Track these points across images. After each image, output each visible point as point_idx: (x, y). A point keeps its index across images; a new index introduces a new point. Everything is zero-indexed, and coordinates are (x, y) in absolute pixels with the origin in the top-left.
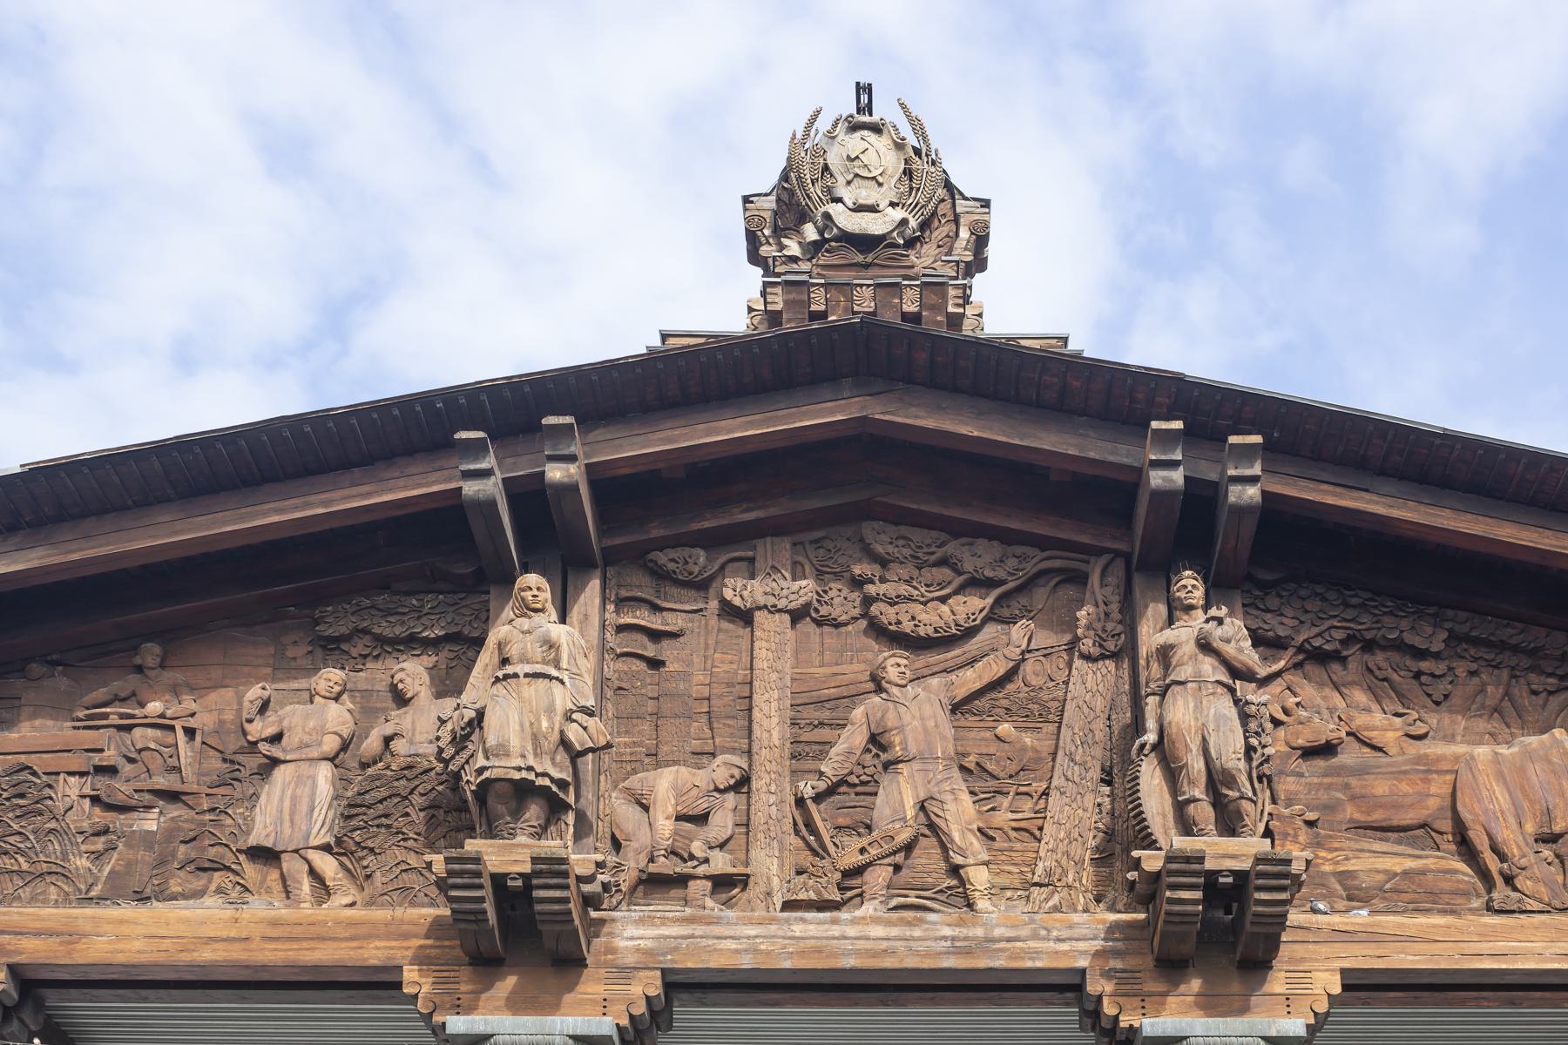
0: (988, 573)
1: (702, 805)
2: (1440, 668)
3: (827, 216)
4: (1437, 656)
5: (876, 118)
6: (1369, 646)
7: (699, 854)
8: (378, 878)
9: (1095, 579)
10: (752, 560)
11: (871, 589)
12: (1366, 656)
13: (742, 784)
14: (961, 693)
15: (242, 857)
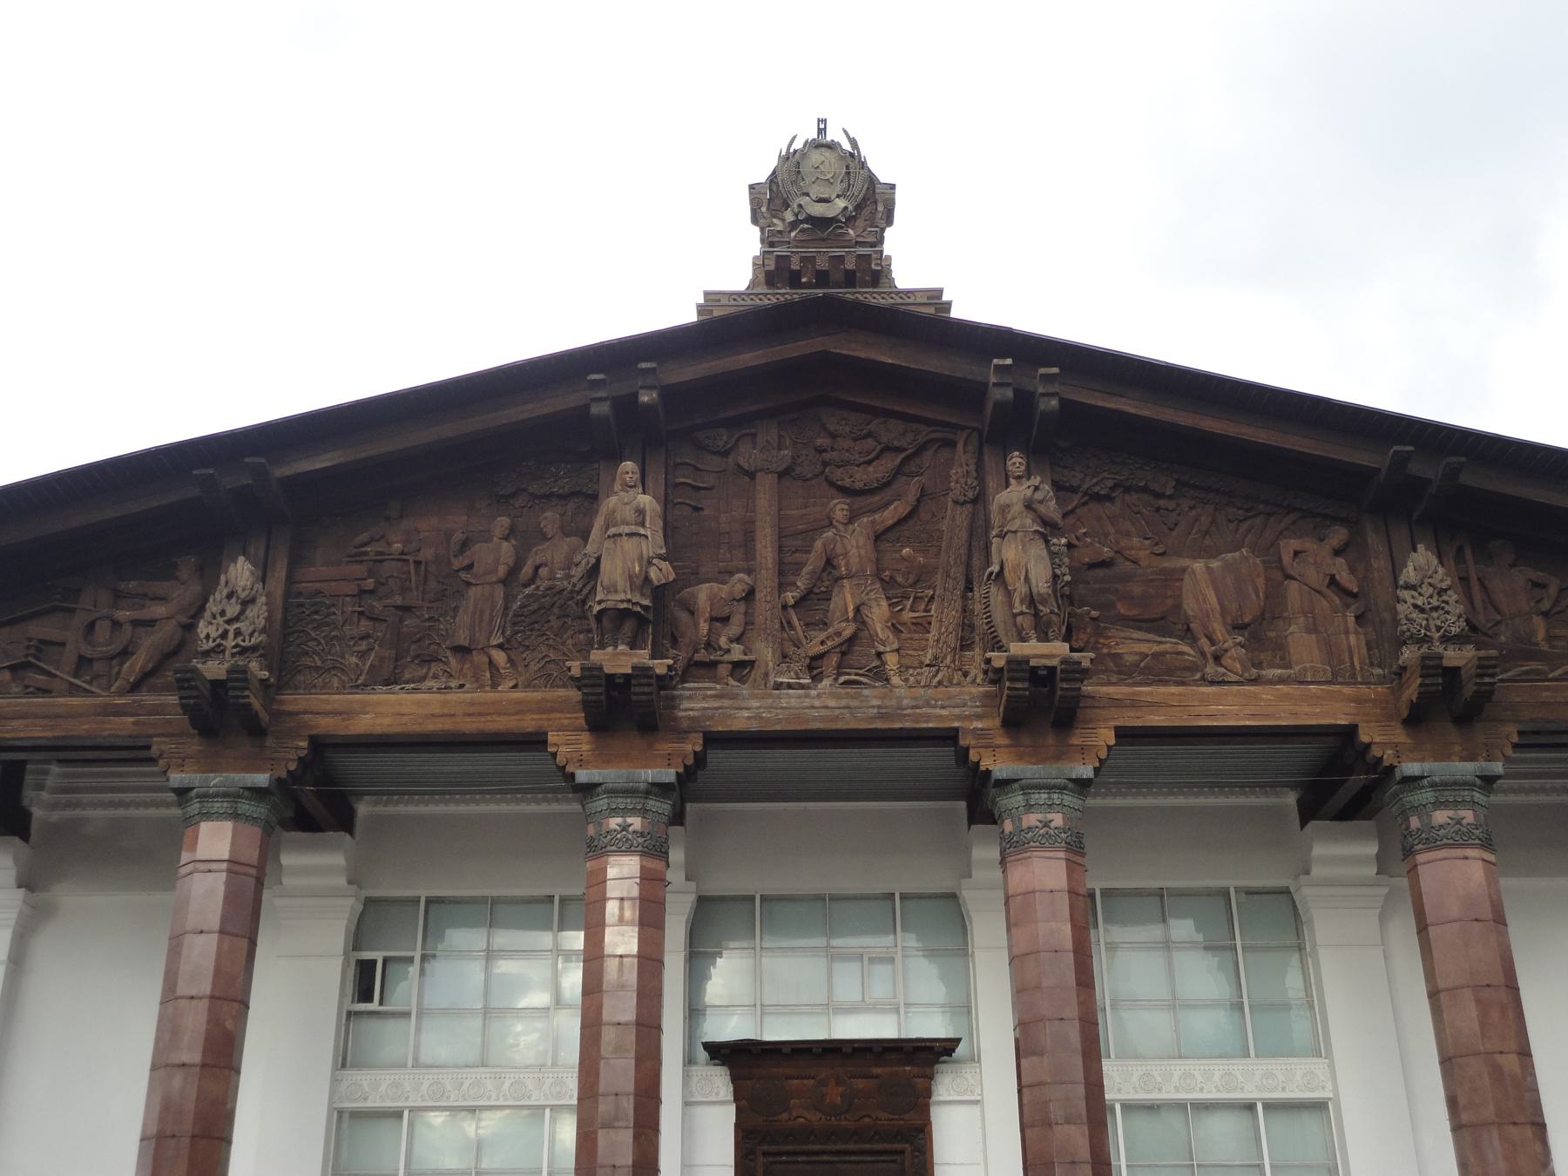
0: (896, 443)
1: (726, 611)
2: (1171, 504)
3: (800, 206)
4: (1170, 497)
5: (829, 138)
6: (1127, 490)
7: (725, 646)
8: (533, 667)
9: (960, 446)
10: (754, 435)
11: (827, 456)
12: (1127, 497)
13: (750, 595)
14: (880, 528)
15: (448, 653)
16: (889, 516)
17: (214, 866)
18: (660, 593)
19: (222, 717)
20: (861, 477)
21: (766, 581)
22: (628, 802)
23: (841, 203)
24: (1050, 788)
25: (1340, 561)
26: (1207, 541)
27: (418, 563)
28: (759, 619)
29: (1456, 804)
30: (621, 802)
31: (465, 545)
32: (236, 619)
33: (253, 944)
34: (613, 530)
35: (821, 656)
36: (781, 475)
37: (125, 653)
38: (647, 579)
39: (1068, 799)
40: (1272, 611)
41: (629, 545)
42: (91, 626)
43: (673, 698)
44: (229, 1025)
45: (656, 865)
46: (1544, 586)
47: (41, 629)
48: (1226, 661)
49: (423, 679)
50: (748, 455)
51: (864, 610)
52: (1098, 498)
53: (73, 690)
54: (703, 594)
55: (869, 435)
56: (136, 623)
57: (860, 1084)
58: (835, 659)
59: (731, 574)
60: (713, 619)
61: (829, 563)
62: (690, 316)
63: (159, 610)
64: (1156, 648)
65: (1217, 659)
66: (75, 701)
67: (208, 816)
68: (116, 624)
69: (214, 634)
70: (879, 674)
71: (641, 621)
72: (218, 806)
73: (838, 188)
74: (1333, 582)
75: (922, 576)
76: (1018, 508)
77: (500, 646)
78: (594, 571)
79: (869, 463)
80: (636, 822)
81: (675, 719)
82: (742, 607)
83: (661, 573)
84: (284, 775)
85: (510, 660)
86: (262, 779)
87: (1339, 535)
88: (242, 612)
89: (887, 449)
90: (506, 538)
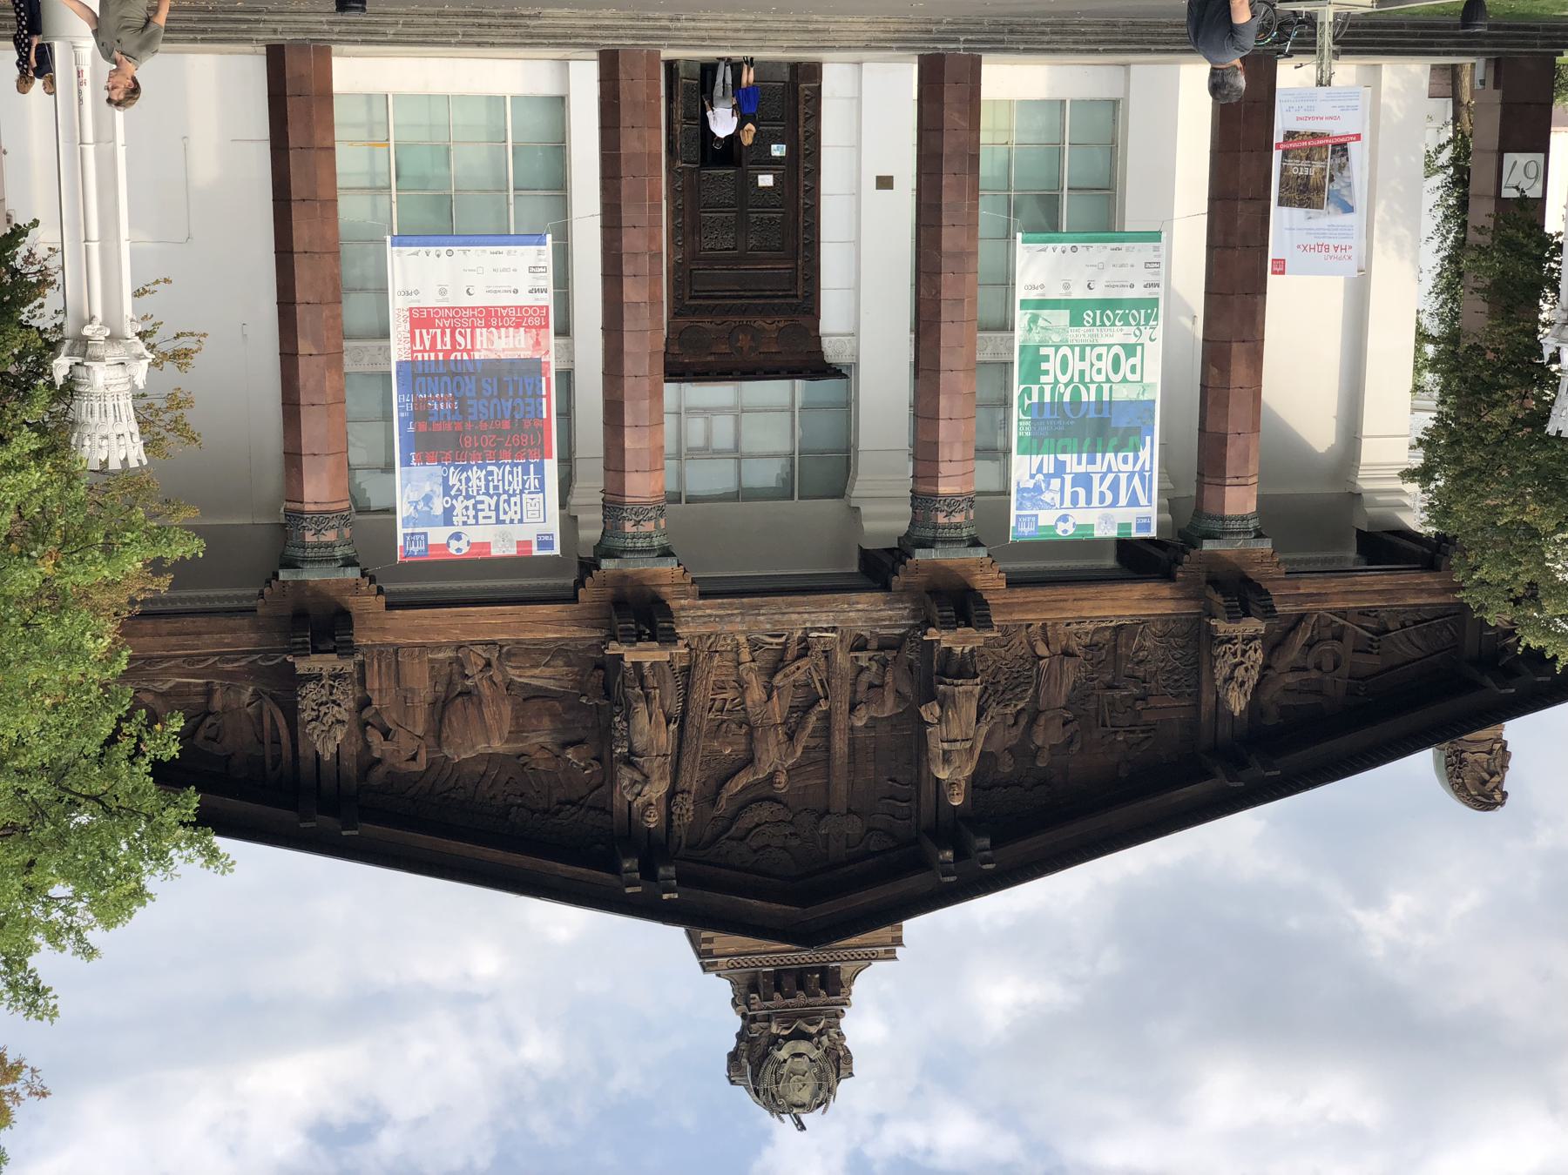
2: (510, 799)
6: (546, 811)
11: (791, 829)
16: (743, 780)
17: (1235, 481)
18: (930, 696)
19: (1240, 591)
20: (764, 812)
21: (840, 721)
22: (947, 534)
23: (783, 1054)
24: (634, 551)
25: (376, 755)
26: (482, 768)
27: (1104, 725)
28: (848, 687)
29: (319, 546)
30: (953, 533)
31: (1070, 742)
32: (1236, 665)
33: (1202, 430)
34: (968, 745)
35: (799, 657)
36: (827, 812)
37: (1309, 645)
38: (941, 707)
39: (619, 543)
40: (441, 708)
41: (955, 733)
42: (1336, 667)
43: (914, 618)
44: (1214, 371)
45: (924, 488)
46: (207, 738)
47: (1370, 662)
48: (481, 663)
49: (1097, 631)
50: (854, 827)
51: (765, 697)
52: (573, 803)
53: (1343, 613)
54: (889, 708)
55: (755, 851)
56: (1305, 669)
57: (724, 348)
58: (789, 657)
59: (866, 726)
60: (882, 686)
61: (791, 737)
62: (913, 927)
63: (1290, 679)
64: (537, 671)
65: (488, 664)
66: (1340, 605)
67: (1243, 518)
68: (1318, 667)
69: (1251, 652)
70: (755, 645)
71: (943, 673)
72: (1236, 526)
73: (785, 1070)
74: (386, 734)
75: (717, 729)
76: (655, 776)
77: (1042, 658)
78: (981, 712)
79: (758, 825)
80: (942, 519)
81: (914, 601)
82: (859, 696)
83: (930, 712)
84: (1192, 551)
85: (1033, 648)
86: (1208, 546)
87: (378, 774)
88: (1233, 671)
89: (742, 839)
90: (1039, 748)
